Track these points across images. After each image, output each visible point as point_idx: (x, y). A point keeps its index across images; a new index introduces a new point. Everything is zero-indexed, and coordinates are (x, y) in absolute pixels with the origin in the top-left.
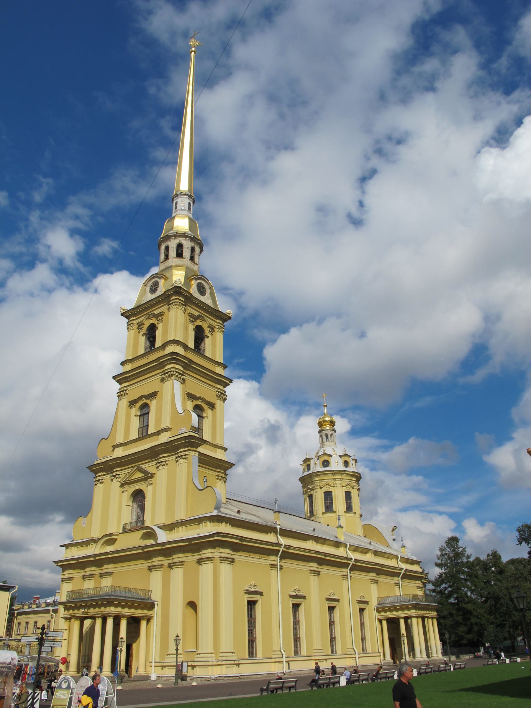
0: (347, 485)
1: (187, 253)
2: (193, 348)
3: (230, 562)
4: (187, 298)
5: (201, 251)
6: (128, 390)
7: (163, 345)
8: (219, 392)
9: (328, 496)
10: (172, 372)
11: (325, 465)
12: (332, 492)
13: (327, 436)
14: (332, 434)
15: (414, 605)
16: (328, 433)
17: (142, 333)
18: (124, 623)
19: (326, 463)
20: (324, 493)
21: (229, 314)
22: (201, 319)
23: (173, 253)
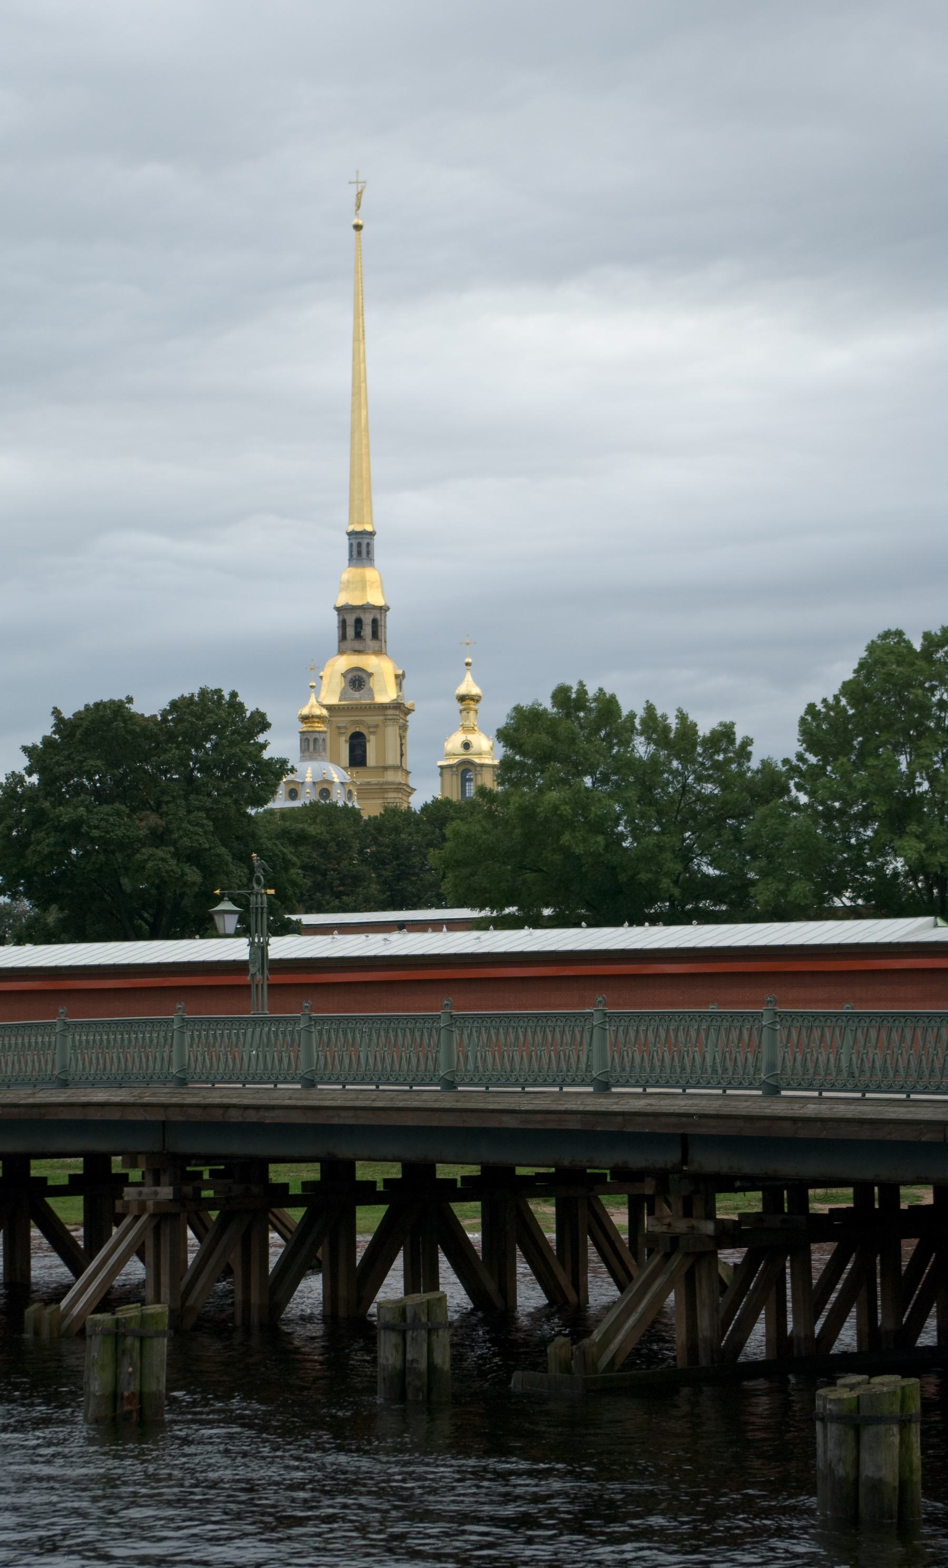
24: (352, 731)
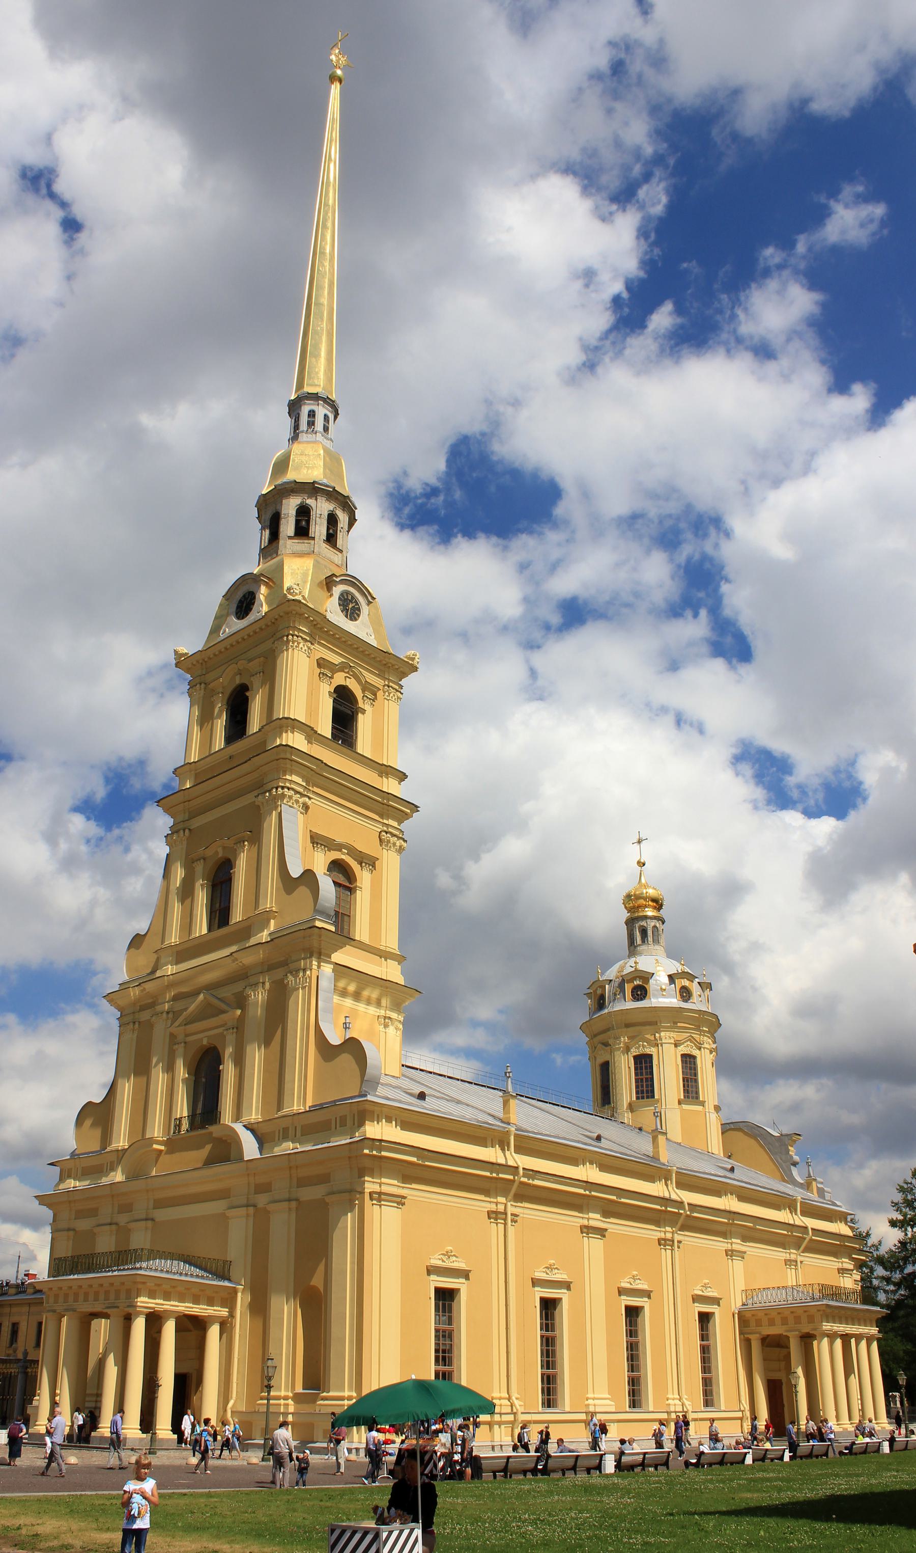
0: (687, 1041)
1: (319, 529)
2: (330, 737)
3: (395, 1205)
4: (315, 625)
5: (352, 521)
6: (189, 829)
7: (260, 730)
8: (387, 833)
9: (644, 1064)
10: (279, 789)
11: (638, 995)
12: (650, 1056)
13: (644, 932)
14: (655, 927)
15: (824, 1308)
16: (645, 925)
18: (169, 1331)
19: (640, 993)
20: (635, 1057)
21: (413, 659)
22: (348, 673)
23: (288, 527)
24: (340, 679)
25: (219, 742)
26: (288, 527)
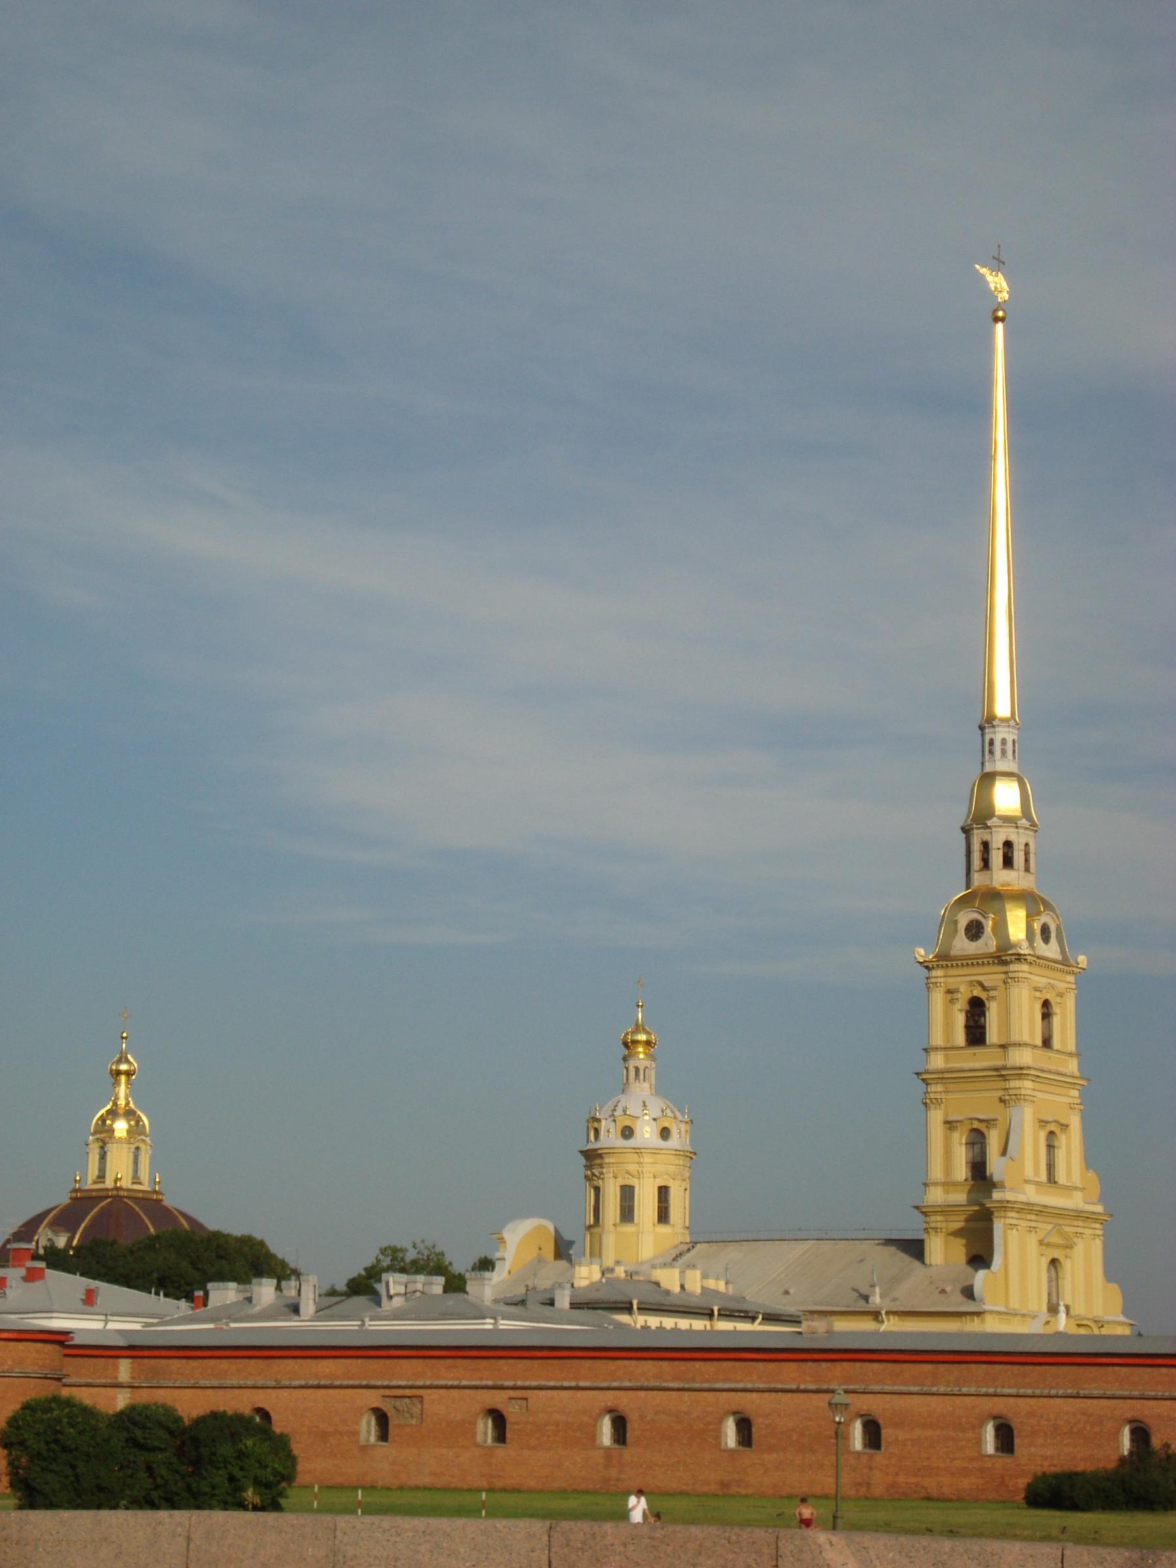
17: (958, 1006)
23: (997, 858)
25: (960, 1038)
26: (997, 858)
